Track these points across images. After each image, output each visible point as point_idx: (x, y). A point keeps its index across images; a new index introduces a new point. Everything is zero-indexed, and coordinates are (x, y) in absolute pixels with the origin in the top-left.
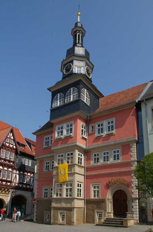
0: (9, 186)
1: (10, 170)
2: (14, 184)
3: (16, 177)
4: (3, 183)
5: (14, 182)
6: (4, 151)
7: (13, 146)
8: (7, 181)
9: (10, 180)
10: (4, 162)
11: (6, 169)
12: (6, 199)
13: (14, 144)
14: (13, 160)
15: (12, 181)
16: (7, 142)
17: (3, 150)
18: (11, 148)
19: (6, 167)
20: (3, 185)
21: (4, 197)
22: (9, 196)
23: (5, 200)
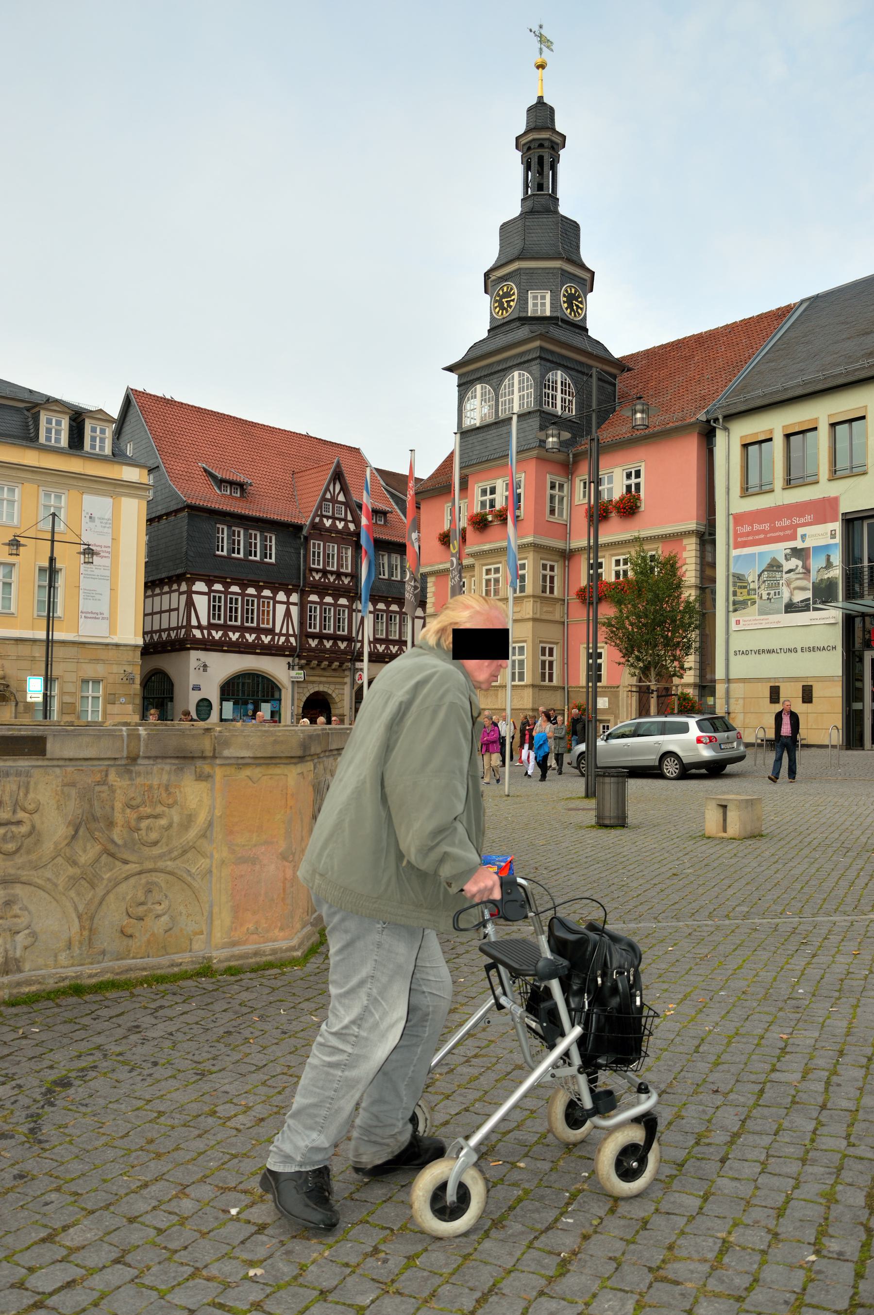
0: (344, 652)
1: (343, 601)
4: (339, 647)
6: (319, 545)
7: (346, 526)
8: (335, 638)
9: (346, 633)
11: (329, 599)
12: (337, 691)
13: (349, 518)
14: (349, 570)
15: (354, 635)
16: (324, 513)
17: (314, 544)
18: (338, 532)
19: (329, 595)
20: (325, 651)
21: (332, 687)
22: (346, 683)
23: (334, 695)
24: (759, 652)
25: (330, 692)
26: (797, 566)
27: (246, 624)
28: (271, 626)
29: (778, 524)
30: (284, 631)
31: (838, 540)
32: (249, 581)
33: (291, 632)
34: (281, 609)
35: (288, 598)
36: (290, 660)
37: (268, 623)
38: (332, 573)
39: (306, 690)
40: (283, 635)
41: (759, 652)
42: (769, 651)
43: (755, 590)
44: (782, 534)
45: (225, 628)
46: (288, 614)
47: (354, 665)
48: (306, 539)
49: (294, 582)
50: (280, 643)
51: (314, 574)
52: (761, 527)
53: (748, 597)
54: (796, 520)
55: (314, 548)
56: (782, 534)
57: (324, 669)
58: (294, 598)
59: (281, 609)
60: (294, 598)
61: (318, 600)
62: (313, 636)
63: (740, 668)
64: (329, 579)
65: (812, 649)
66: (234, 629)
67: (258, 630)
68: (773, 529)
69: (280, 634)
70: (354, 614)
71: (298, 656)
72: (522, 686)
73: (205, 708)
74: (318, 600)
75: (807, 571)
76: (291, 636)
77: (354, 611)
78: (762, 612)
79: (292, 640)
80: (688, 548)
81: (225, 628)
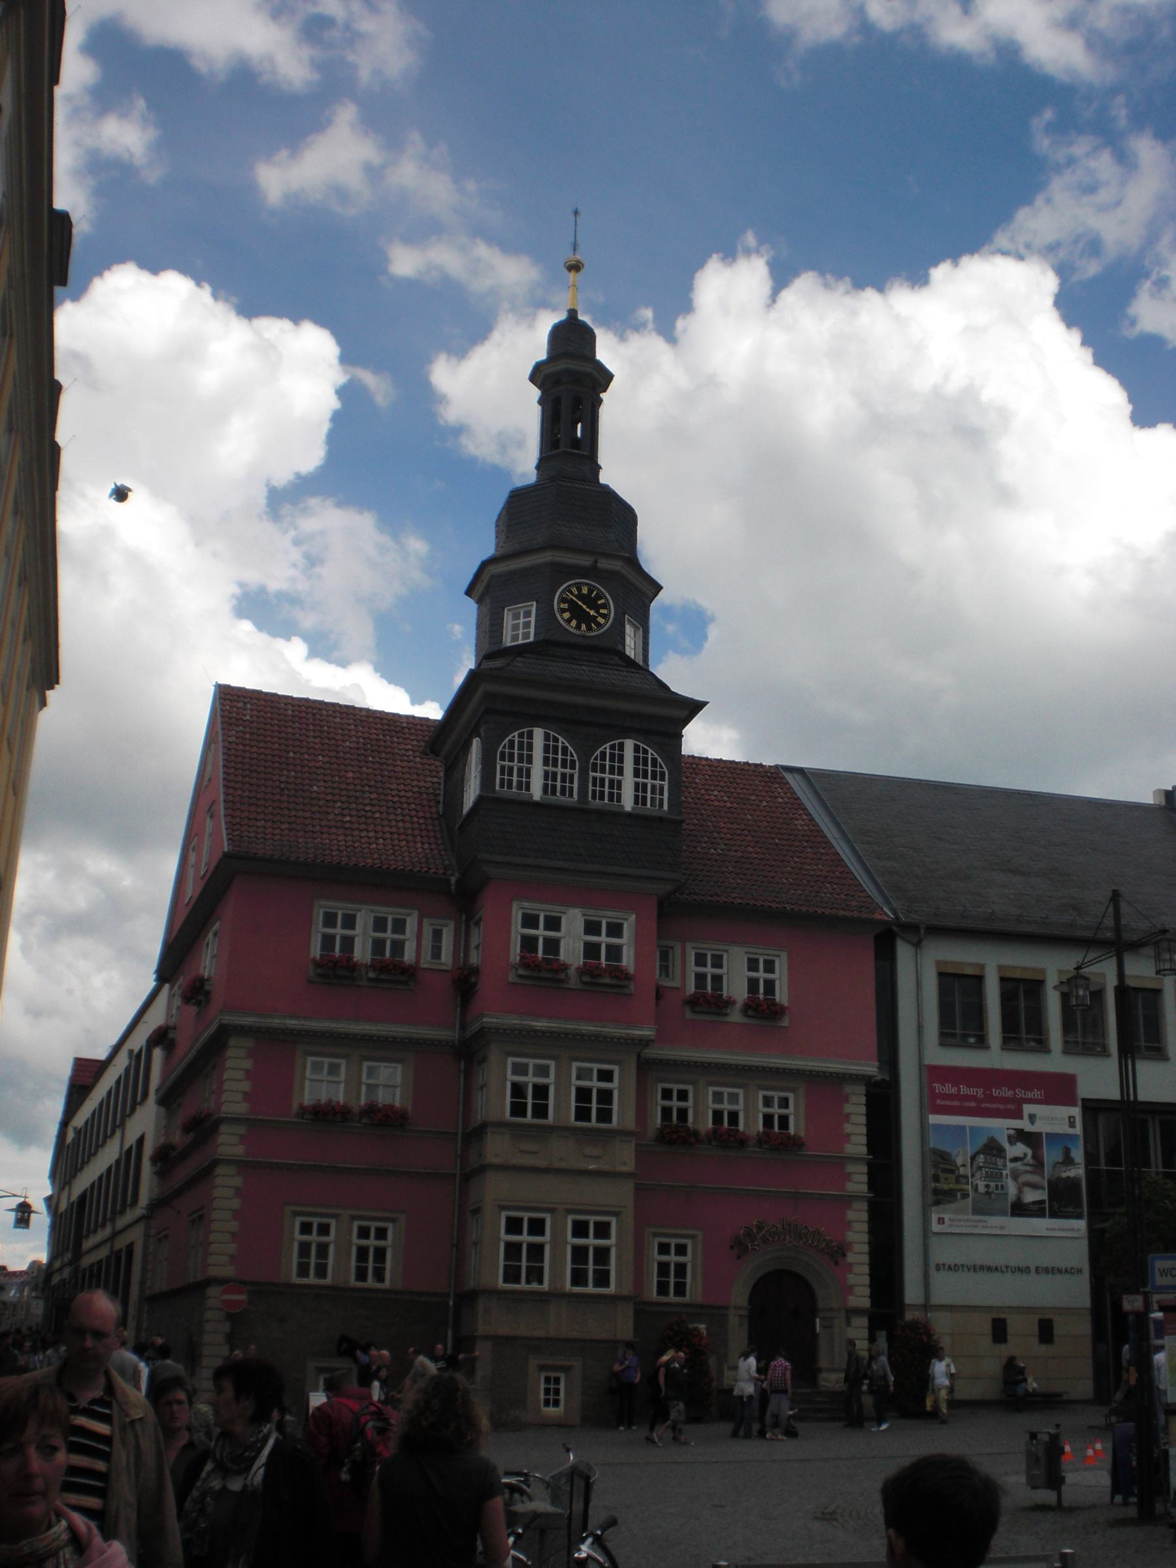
24: (975, 1268)
26: (1026, 1155)
29: (995, 1093)
31: (1078, 1130)
41: (975, 1268)
42: (989, 1269)
43: (966, 1177)
44: (1001, 1107)
52: (971, 1091)
53: (958, 1187)
54: (1020, 1093)
56: (1001, 1107)
63: (946, 1289)
65: (1047, 1271)
68: (989, 1098)
75: (1039, 1163)
78: (977, 1211)
80: (854, 1099)
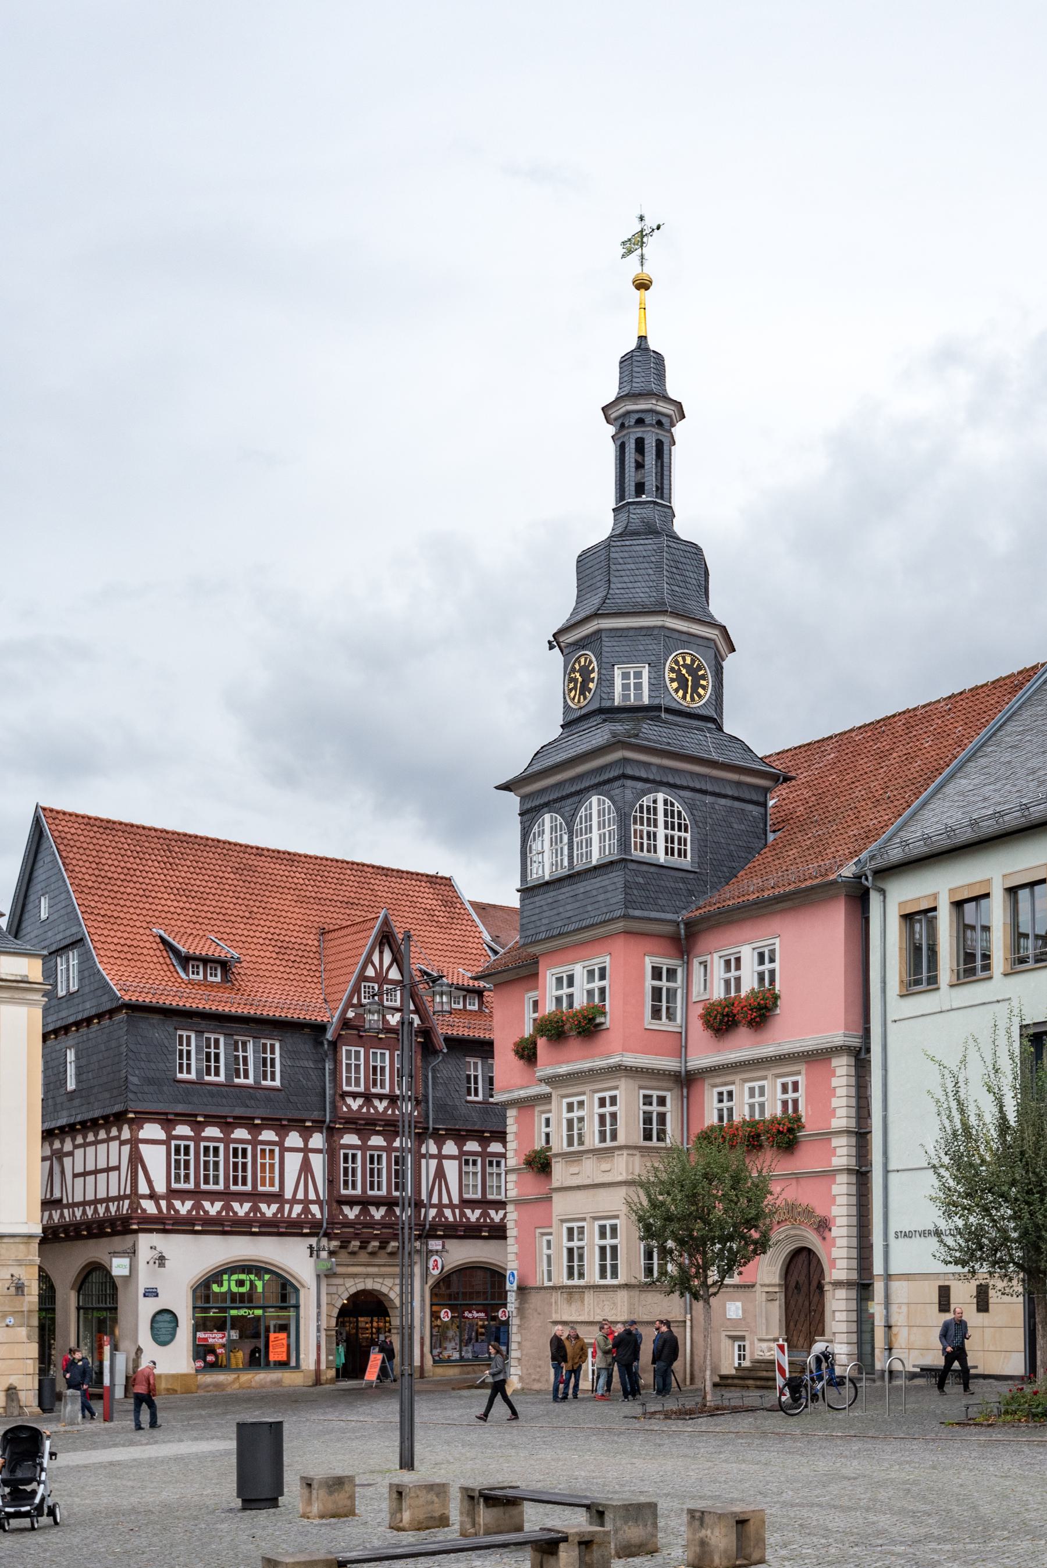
2: (433, 1212)
3: (440, 1173)
5: (435, 1200)
6: (357, 1053)
10: (364, 1110)
11: (377, 1141)
15: (424, 1196)
17: (348, 1052)
19: (378, 1133)
20: (372, 1224)
25: (385, 1290)
27: (233, 1188)
28: (276, 1189)
30: (300, 1196)
32: (235, 1118)
33: (312, 1196)
34: (293, 1162)
35: (306, 1142)
36: (313, 1241)
37: (272, 1185)
38: (381, 1097)
39: (341, 1289)
40: (299, 1202)
45: (196, 1194)
46: (306, 1167)
47: (427, 1245)
48: (334, 1045)
49: (316, 1115)
50: (294, 1215)
51: (349, 1101)
55: (349, 1058)
57: (373, 1254)
58: (317, 1140)
59: (293, 1162)
60: (317, 1140)
61: (359, 1143)
62: (351, 1202)
64: (375, 1108)
66: (213, 1196)
67: (255, 1197)
69: (294, 1201)
70: (424, 1161)
71: (326, 1235)
72: (613, 1286)
73: (166, 1325)
74: (359, 1143)
76: (313, 1202)
77: (424, 1156)
79: (315, 1209)
81: (196, 1194)
